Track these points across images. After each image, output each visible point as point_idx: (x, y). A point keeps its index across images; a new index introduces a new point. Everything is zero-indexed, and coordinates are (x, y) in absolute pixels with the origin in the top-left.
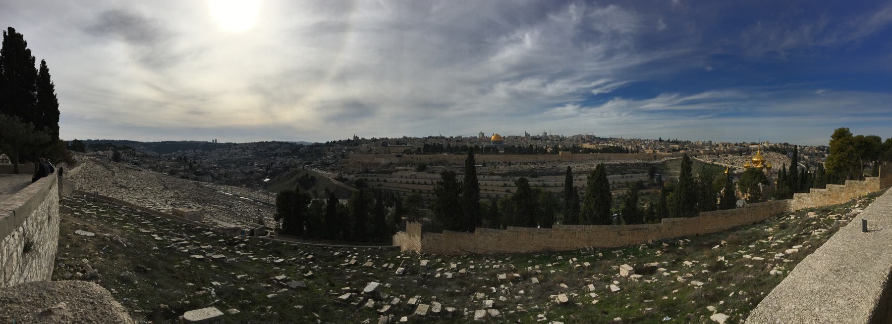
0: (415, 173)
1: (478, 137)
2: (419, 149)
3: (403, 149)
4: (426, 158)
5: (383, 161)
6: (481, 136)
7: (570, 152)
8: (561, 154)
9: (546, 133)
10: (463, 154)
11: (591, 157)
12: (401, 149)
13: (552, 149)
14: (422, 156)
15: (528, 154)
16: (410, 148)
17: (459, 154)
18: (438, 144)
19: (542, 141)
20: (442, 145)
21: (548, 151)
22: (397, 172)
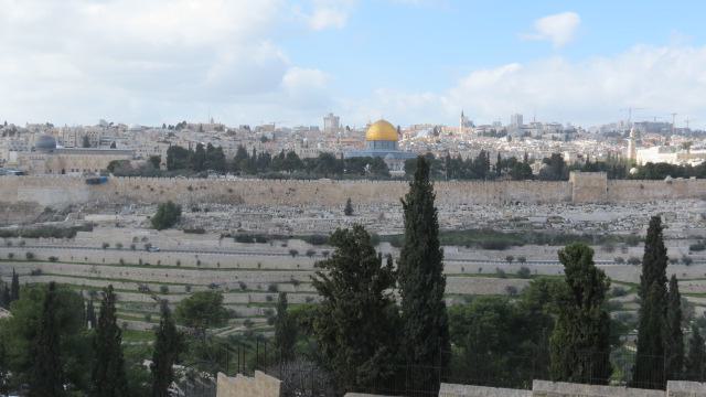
0: (146, 233)
1: (321, 129)
2: (155, 160)
3: (104, 160)
4: (176, 188)
5: (45, 196)
6: (330, 124)
7: (603, 176)
8: (576, 179)
9: (520, 118)
10: (287, 178)
11: (668, 191)
12: (99, 162)
13: (544, 165)
14: (167, 182)
15: (476, 178)
16: (125, 157)
17: (271, 177)
18: (210, 146)
19: (510, 139)
20: (220, 149)
21: (535, 172)
22: (91, 230)
